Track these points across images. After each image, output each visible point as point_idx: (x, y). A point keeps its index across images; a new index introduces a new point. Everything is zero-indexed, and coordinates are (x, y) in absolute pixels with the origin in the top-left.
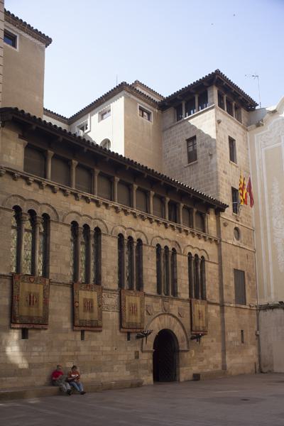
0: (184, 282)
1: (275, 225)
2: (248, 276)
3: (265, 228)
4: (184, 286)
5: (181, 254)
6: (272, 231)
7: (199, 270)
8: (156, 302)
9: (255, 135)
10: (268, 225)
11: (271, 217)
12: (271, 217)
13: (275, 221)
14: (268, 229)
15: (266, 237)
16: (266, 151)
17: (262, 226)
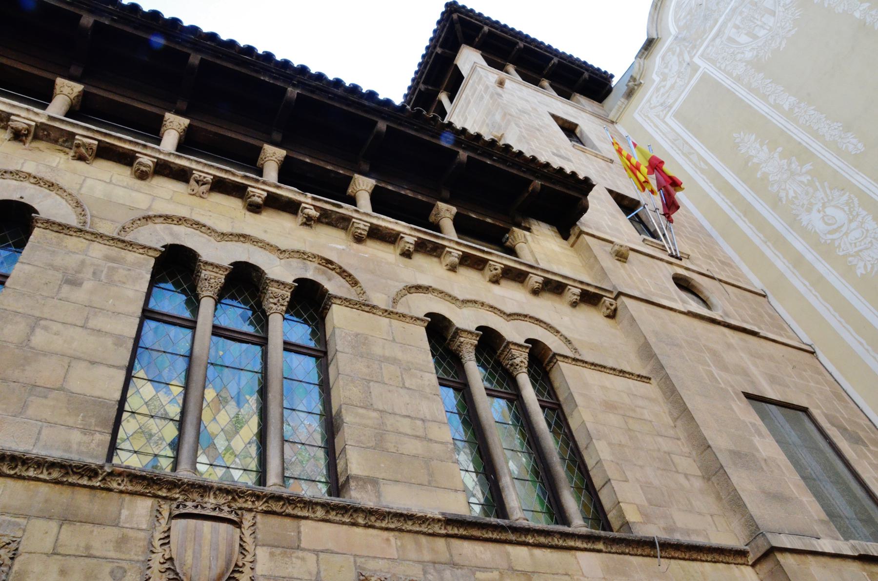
0: (405, 426)
1: (820, 226)
2: (843, 430)
3: (798, 261)
4: (413, 447)
5: (371, 308)
6: (827, 251)
7: (529, 393)
8: (66, 519)
9: (636, 116)
10: (799, 245)
11: (794, 222)
12: (794, 222)
13: (815, 221)
14: (810, 256)
15: (818, 282)
16: (678, 116)
17: (781, 264)
